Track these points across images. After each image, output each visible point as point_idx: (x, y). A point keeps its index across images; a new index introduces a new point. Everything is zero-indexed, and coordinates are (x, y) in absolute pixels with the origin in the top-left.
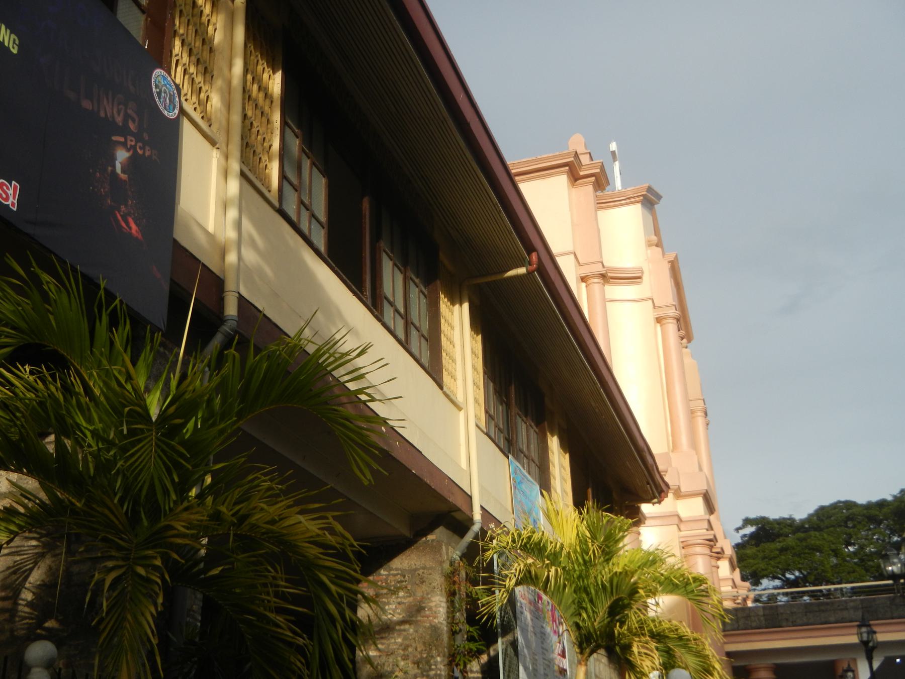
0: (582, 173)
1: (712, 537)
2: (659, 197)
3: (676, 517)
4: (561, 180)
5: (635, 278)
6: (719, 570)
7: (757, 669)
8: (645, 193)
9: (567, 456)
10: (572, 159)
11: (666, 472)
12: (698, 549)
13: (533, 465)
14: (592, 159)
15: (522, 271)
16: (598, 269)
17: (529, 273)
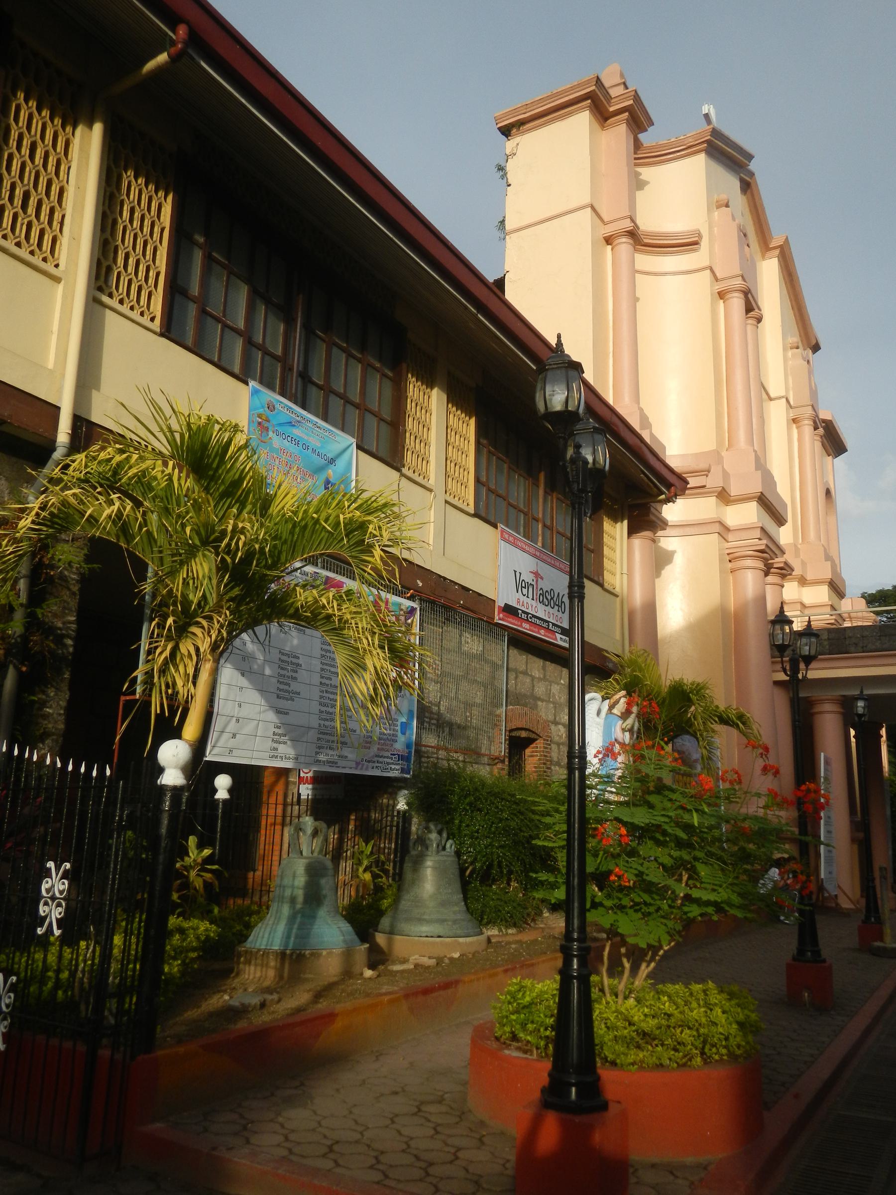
0: (611, 109)
1: (763, 547)
2: (750, 157)
3: (717, 524)
4: (583, 119)
5: (690, 244)
6: (784, 589)
7: (822, 701)
8: (709, 137)
9: (473, 421)
10: (594, 87)
11: (709, 471)
12: (749, 562)
13: (372, 422)
14: (626, 88)
15: (163, 58)
16: (627, 224)
17: (174, 59)
